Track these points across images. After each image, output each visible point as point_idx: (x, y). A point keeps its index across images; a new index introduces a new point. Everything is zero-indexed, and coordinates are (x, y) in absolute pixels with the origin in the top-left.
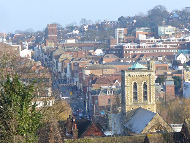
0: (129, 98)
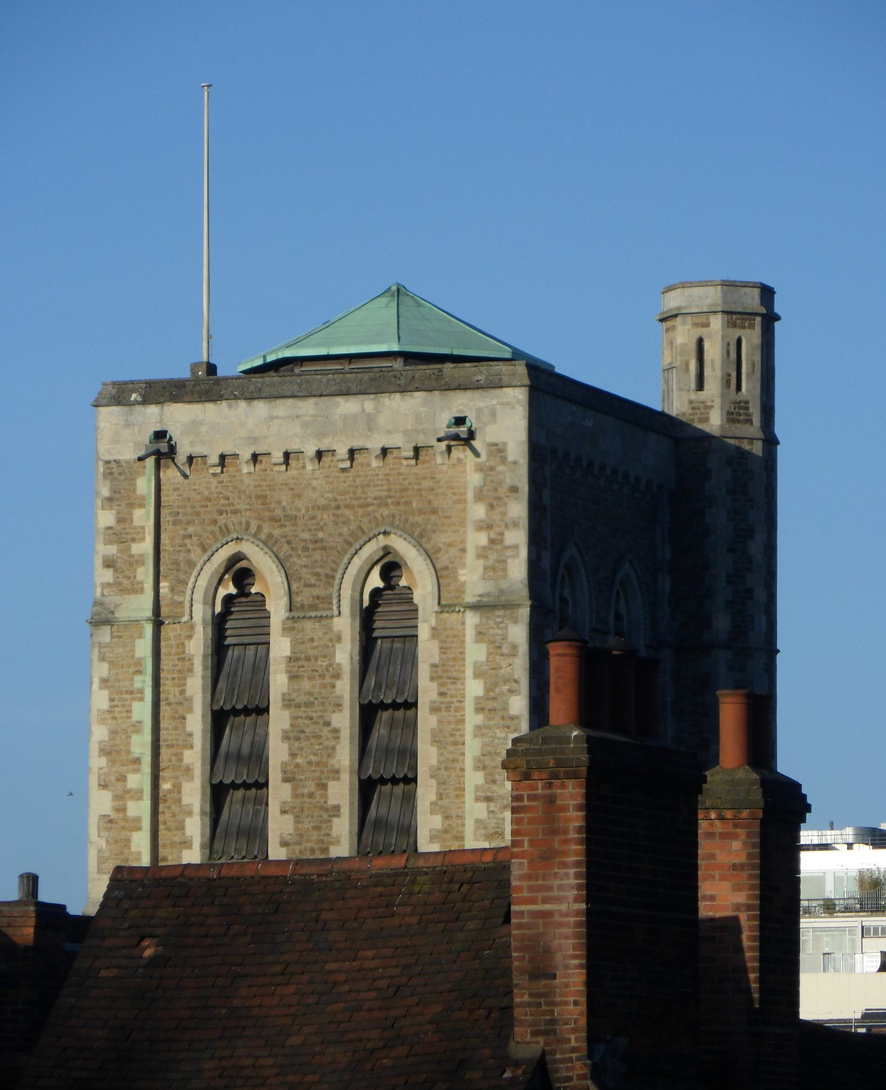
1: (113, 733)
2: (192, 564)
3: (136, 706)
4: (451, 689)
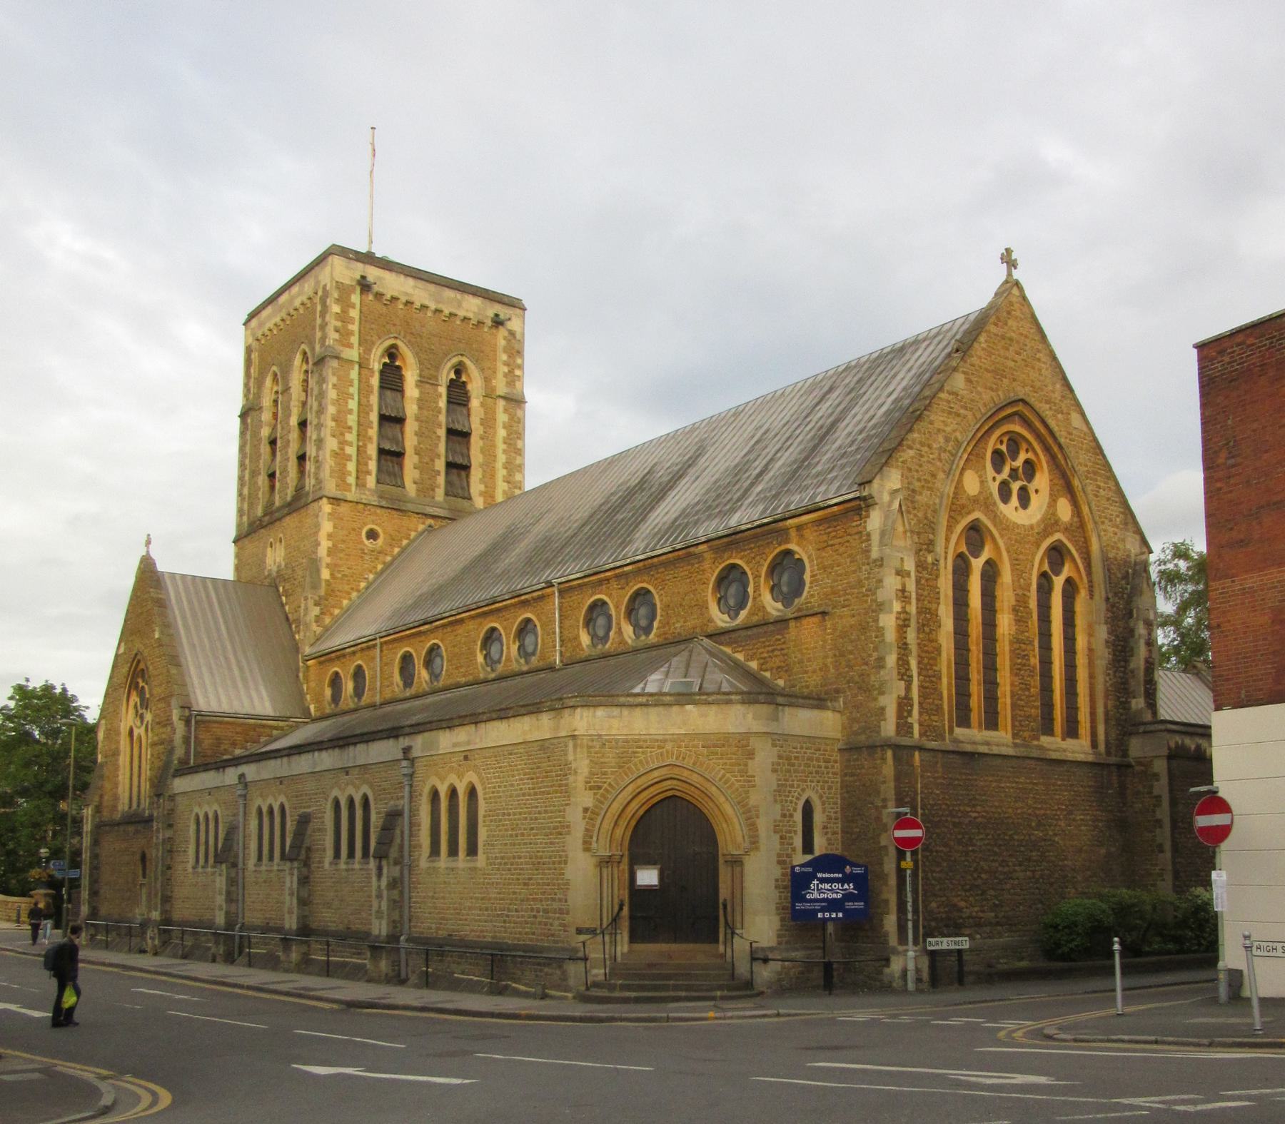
0: (351, 450)
1: (339, 412)
2: (373, 343)
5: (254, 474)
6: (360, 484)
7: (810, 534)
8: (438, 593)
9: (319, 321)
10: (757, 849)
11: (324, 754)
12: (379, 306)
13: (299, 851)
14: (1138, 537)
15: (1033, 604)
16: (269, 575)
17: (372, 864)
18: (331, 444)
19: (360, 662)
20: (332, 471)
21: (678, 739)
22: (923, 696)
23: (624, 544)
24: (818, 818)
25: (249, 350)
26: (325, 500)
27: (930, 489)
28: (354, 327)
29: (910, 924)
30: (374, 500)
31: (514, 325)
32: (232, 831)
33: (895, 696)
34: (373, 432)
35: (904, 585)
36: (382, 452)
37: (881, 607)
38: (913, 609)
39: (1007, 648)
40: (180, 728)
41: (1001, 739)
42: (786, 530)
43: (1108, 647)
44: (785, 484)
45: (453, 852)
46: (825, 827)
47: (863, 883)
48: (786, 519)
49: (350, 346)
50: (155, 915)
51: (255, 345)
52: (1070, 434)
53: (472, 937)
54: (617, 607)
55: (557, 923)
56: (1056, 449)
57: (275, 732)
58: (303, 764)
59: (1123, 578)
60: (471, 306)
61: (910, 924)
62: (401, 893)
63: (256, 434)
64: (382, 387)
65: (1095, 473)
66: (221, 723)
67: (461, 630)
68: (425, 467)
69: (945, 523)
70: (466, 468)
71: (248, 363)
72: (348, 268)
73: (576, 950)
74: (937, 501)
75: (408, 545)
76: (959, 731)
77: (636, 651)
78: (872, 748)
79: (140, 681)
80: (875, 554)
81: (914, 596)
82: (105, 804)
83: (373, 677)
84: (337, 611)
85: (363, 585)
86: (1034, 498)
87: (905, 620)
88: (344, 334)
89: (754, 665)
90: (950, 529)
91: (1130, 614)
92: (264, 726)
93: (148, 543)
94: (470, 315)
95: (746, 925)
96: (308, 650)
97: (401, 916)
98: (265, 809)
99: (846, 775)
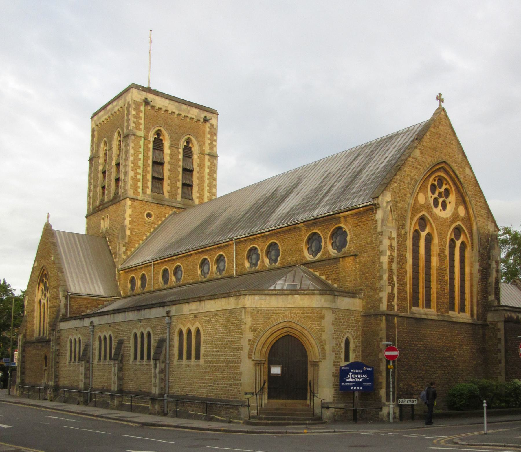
0: (140, 177)
1: (134, 159)
2: (150, 129)
3: (140, 155)
4: (201, 169)
5: (95, 186)
6: (144, 192)
7: (348, 219)
8: (179, 242)
9: (126, 118)
10: (325, 359)
11: (130, 314)
12: (153, 112)
13: (118, 356)
14: (493, 224)
15: (447, 253)
16: (102, 232)
17: (152, 362)
18: (131, 174)
19: (144, 272)
20: (131, 186)
21: (291, 310)
22: (399, 293)
23: (266, 222)
24: (352, 346)
25: (93, 131)
26: (128, 199)
27: (403, 201)
28: (142, 121)
29: (391, 393)
30: (150, 200)
31: (213, 121)
32: (87, 346)
33: (387, 293)
34: (150, 169)
35: (391, 244)
36: (154, 178)
37: (381, 253)
38: (395, 254)
39: (435, 272)
40: (63, 300)
41: (432, 312)
42: (339, 218)
43: (479, 272)
44: (338, 198)
45: (189, 357)
46: (354, 350)
47: (372, 375)
48: (339, 213)
49: (140, 130)
50: (51, 383)
51: (96, 128)
52: (465, 177)
53: (197, 395)
54: (262, 250)
55: (236, 390)
56: (459, 184)
57: (105, 303)
58: (120, 317)
59: (487, 242)
60: (194, 113)
61: (391, 393)
62: (165, 376)
63: (96, 169)
64: (154, 149)
65: (475, 195)
66: (81, 298)
67: (190, 259)
68: (173, 185)
69: (410, 216)
70: (191, 186)
71: (93, 136)
72: (139, 94)
73: (245, 402)
74: (407, 206)
75: (165, 220)
76: (414, 309)
77: (270, 270)
78: (376, 315)
79: (44, 279)
80: (379, 230)
81: (396, 248)
82: (28, 333)
83: (150, 279)
84: (133, 249)
85: (145, 238)
86: (448, 205)
87: (392, 259)
88: (137, 124)
89: (323, 277)
90: (412, 219)
91: (489, 258)
92: (100, 300)
93: (48, 217)
94: (194, 117)
95: (319, 392)
96: (120, 267)
97: (165, 386)
98: (102, 337)
99: (364, 327)
